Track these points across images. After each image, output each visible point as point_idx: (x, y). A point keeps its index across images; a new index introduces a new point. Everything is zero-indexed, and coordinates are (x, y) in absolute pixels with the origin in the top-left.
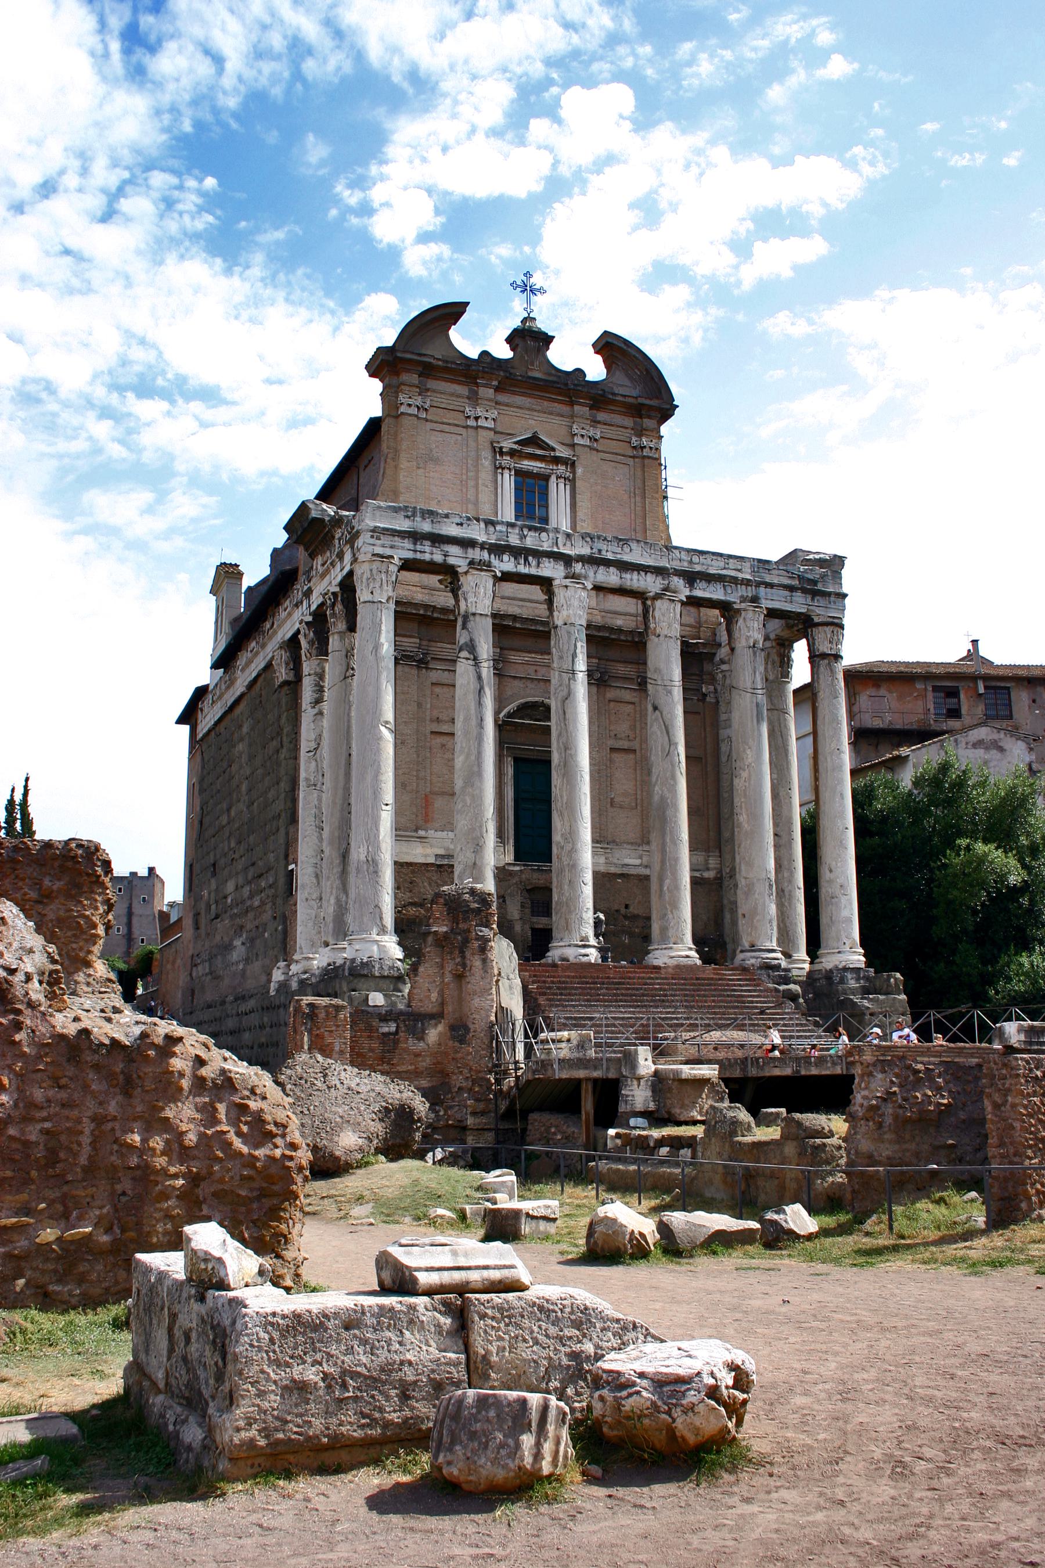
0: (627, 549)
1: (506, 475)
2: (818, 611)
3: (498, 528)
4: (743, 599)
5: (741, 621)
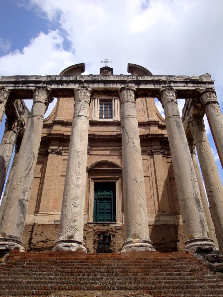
0: (107, 77)
1: (96, 100)
2: (201, 88)
3: (52, 77)
4: (163, 87)
5: (164, 95)
